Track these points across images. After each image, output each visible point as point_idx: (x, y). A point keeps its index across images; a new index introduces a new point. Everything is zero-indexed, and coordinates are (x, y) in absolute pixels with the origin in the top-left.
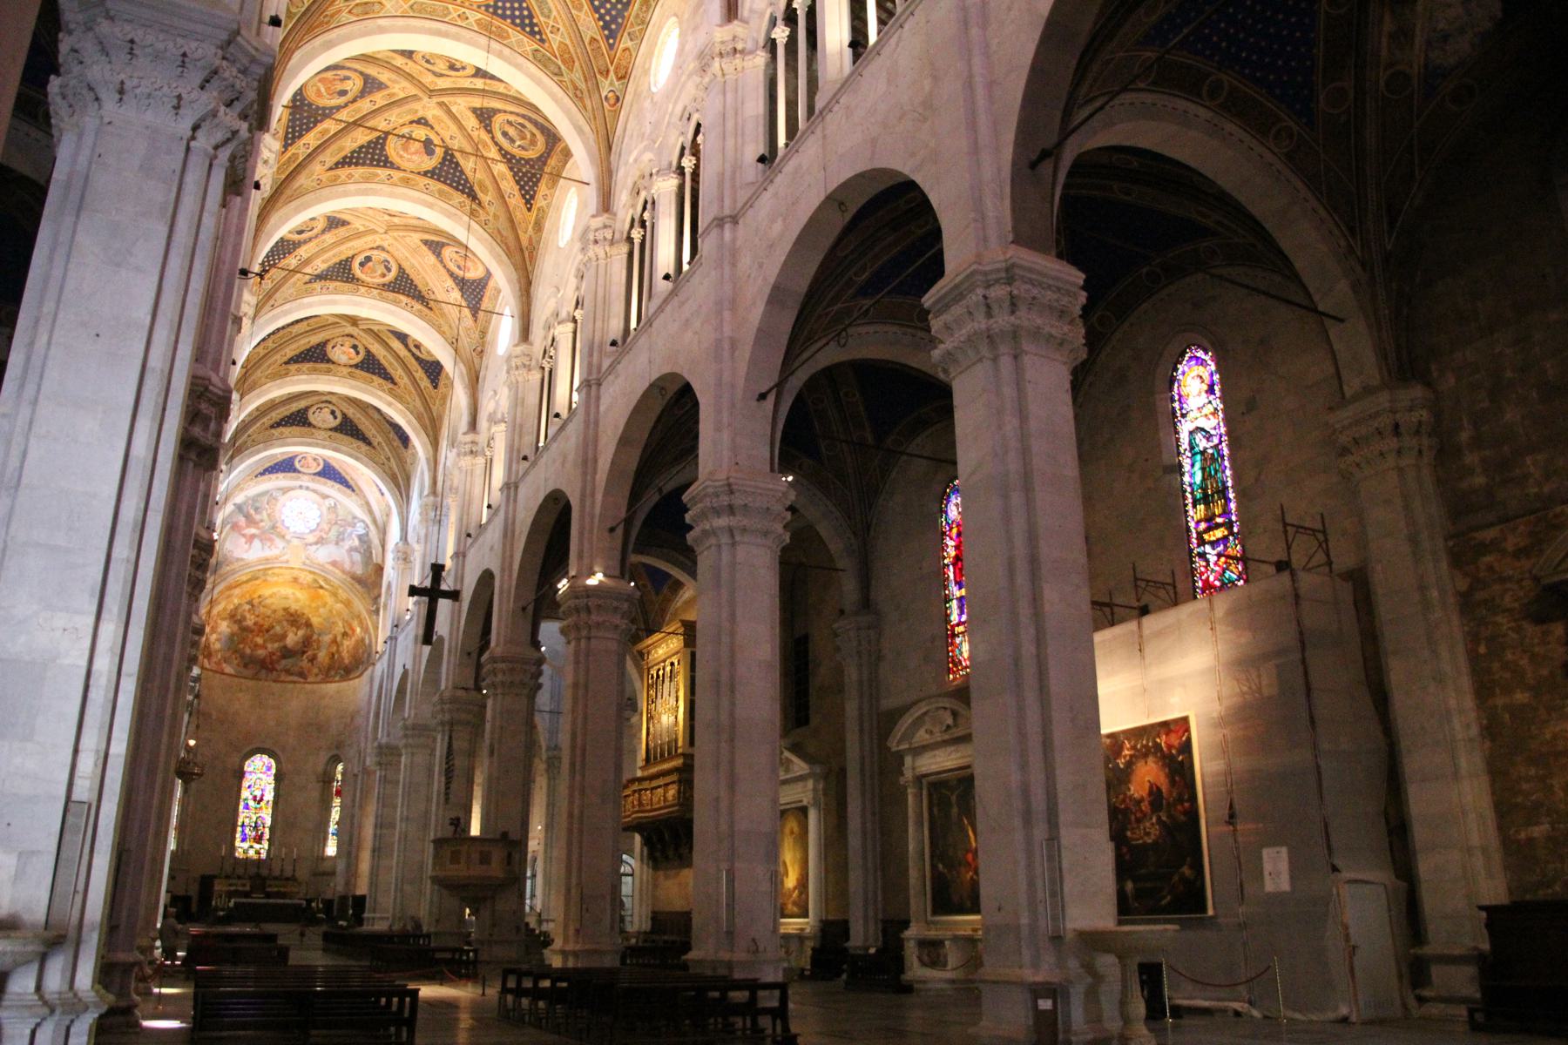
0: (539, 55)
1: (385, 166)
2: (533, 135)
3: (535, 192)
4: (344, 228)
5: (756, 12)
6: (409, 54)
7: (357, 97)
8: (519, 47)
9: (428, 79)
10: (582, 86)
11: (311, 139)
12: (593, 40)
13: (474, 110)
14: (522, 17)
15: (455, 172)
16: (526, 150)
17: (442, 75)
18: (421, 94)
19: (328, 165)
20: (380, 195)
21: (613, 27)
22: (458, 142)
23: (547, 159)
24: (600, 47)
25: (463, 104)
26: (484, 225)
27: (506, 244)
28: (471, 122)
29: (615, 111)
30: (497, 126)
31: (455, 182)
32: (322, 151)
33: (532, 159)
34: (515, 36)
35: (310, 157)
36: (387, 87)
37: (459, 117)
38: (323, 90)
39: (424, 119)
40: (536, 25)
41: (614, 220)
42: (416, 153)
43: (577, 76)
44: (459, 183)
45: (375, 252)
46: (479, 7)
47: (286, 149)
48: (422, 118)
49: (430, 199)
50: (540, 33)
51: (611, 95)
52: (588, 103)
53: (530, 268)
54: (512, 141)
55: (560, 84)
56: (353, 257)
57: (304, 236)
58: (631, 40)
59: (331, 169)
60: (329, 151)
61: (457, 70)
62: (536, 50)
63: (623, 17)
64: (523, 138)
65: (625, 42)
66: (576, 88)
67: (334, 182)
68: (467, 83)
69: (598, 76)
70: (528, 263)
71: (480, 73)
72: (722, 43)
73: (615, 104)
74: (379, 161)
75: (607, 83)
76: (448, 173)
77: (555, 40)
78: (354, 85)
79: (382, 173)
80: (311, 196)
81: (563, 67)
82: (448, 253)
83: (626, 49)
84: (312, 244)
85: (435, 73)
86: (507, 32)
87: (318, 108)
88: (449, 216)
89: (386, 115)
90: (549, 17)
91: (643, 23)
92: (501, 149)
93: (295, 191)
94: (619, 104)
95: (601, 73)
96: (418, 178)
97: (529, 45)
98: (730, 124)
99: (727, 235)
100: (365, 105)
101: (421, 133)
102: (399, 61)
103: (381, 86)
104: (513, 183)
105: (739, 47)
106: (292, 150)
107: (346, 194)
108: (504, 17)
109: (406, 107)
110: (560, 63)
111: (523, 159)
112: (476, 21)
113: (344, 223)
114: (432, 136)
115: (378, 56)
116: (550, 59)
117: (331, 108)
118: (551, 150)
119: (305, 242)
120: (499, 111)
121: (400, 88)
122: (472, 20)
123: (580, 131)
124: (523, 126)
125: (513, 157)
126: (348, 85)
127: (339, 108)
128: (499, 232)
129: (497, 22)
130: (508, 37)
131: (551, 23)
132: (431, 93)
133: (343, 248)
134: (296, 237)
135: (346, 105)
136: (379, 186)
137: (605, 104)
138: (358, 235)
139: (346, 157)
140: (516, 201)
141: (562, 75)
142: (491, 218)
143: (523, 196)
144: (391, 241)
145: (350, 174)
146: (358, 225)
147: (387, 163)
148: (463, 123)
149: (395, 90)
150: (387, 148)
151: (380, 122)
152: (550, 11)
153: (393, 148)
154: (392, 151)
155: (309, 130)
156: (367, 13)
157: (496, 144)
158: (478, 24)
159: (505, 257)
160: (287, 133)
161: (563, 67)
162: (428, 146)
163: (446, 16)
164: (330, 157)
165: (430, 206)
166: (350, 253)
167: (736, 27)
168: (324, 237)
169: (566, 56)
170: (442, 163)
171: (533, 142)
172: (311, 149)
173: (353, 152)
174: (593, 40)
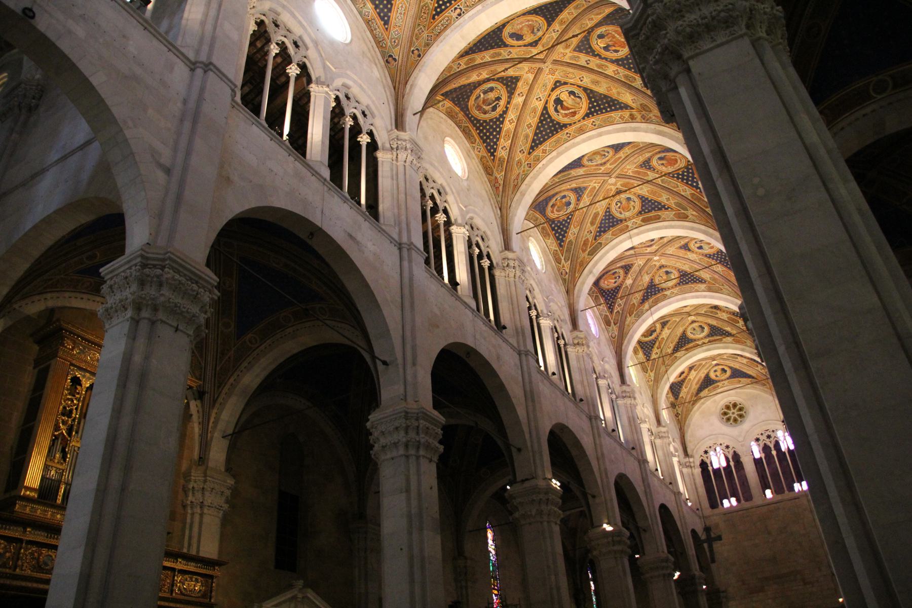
2: (485, 113)
16: (475, 99)
23: (465, 114)
33: (468, 101)
36: (575, 50)
42: (521, 29)
48: (536, 46)
54: (485, 92)
64: (484, 101)
101: (529, 39)
114: (520, 43)
118: (470, 119)
149: (568, 51)
150: (543, 19)
154: (537, 19)
162: (518, 37)
171: (479, 108)
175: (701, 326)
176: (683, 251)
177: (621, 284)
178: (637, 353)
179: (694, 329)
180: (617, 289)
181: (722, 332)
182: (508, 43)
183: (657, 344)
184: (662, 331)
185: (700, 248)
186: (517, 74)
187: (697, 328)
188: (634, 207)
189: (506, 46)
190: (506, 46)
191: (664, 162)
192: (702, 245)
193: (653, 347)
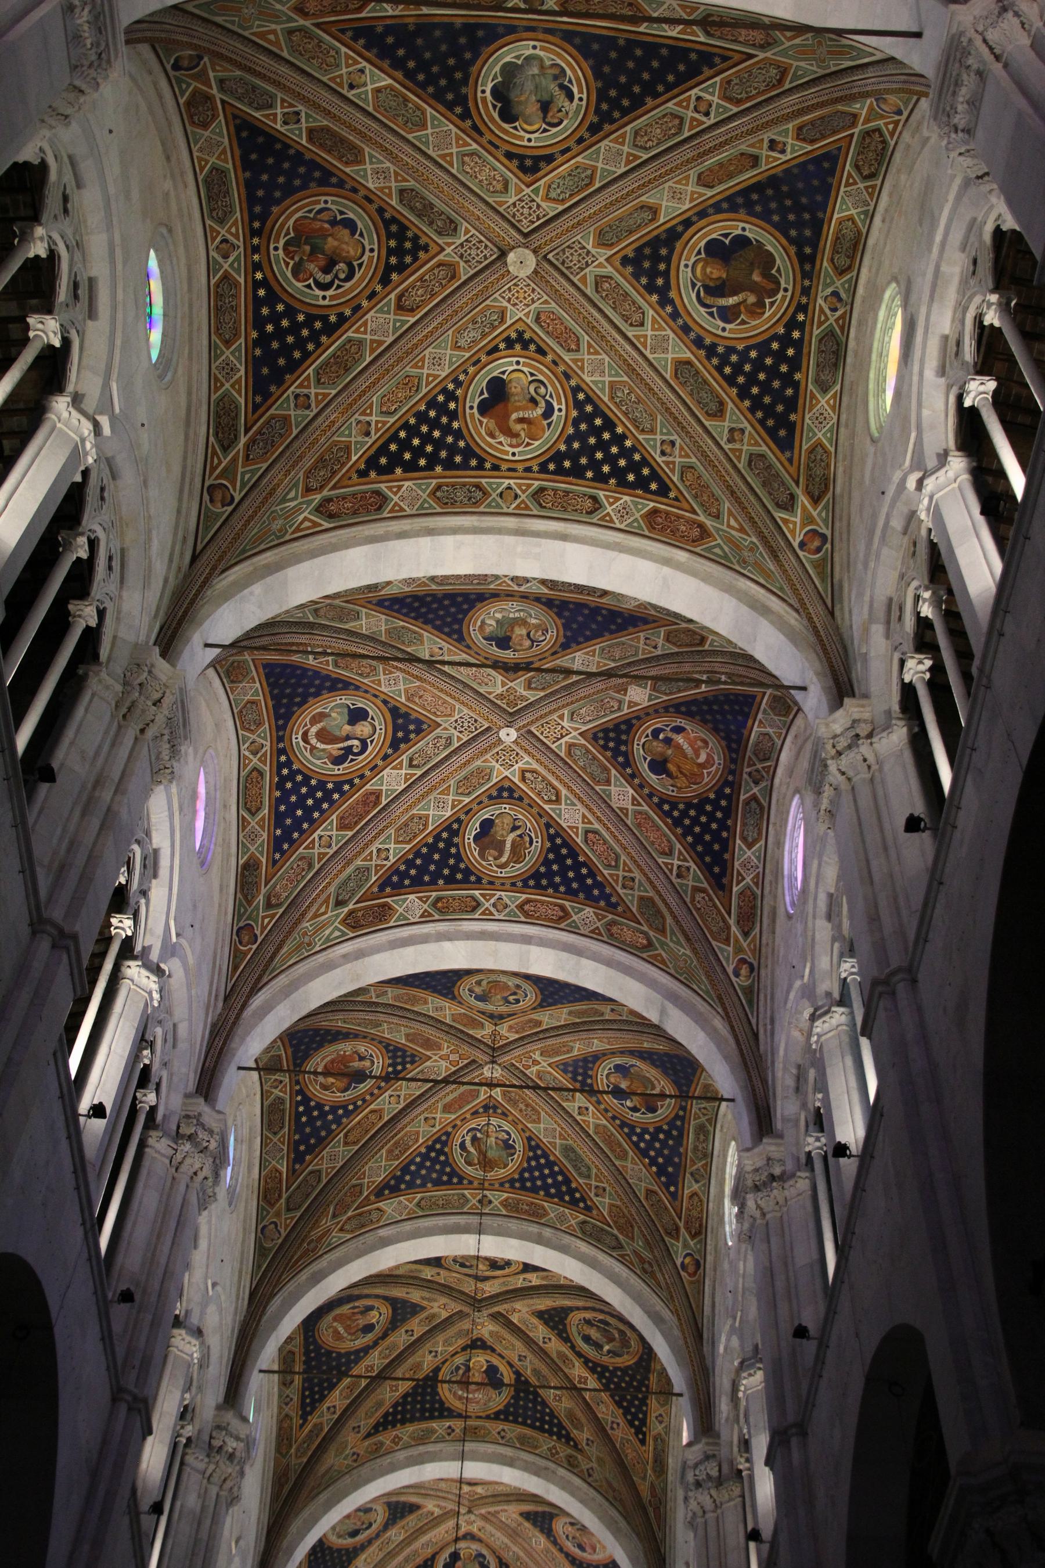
0: (588, 1228)
1: (441, 1416)
2: (622, 1333)
3: (645, 1414)
4: (412, 1517)
5: (789, 1120)
6: (436, 1262)
7: (388, 1329)
8: (562, 1222)
9: (469, 1286)
10: (647, 1255)
11: (337, 1399)
12: (649, 1192)
13: (540, 1315)
14: (556, 1184)
15: (535, 1407)
17: (486, 1279)
18: (466, 1309)
19: (363, 1431)
20: (441, 1460)
21: (670, 1169)
22: (530, 1365)
24: (660, 1200)
25: (525, 1310)
26: (586, 1476)
27: (621, 1501)
28: (540, 1331)
29: (698, 1281)
30: (574, 1329)
31: (538, 1420)
32: (353, 1412)
33: (629, 1367)
34: (553, 1209)
35: (338, 1424)
36: (423, 1308)
37: (523, 1328)
38: (341, 1330)
39: (480, 1339)
40: (576, 1190)
41: (718, 1444)
43: (639, 1244)
44: (543, 1421)
45: (462, 1545)
46: (502, 1185)
47: (305, 1420)
48: (478, 1339)
49: (509, 1452)
50: (583, 1199)
51: (687, 1260)
52: (659, 1275)
53: (659, 1535)
54: (598, 1346)
55: (622, 1260)
56: (433, 1557)
57: (361, 1537)
58: (697, 1181)
59: (369, 1435)
60: (361, 1412)
61: (502, 1268)
62: (584, 1222)
63: (680, 1155)
64: (611, 1340)
65: (690, 1186)
66: (642, 1260)
67: (377, 1452)
68: (519, 1282)
69: (666, 1239)
70: (655, 1527)
71: (528, 1268)
72: (756, 1170)
73: (695, 1273)
74: (432, 1410)
75: (680, 1245)
76: (525, 1408)
77: (603, 1203)
78: (380, 1315)
79: (439, 1426)
80: (347, 1480)
81: (621, 1237)
82: (559, 1526)
83: (694, 1194)
84: (371, 1550)
85: (478, 1278)
86: (543, 1207)
87: (339, 1354)
88: (537, 1472)
89: (428, 1346)
90: (589, 1177)
91: (705, 1156)
92: (586, 1361)
93: (324, 1475)
94: (701, 1270)
95: (669, 1234)
96: (488, 1424)
97: (574, 1218)
98: (780, 1284)
99: (796, 1456)
100: (400, 1339)
101: (480, 1360)
102: (428, 1273)
103: (415, 1309)
104: (612, 1407)
105: (777, 1171)
106: (313, 1420)
107: (393, 1468)
108: (534, 1190)
109: (451, 1331)
110: (615, 1232)
111: (619, 1369)
112: (501, 1203)
113: (413, 1508)
114: (495, 1361)
115: (397, 1272)
116: (602, 1230)
117: (357, 1352)
119: (363, 1547)
120: (571, 1309)
121: (440, 1307)
122: (496, 1203)
123: (657, 1319)
124: (607, 1324)
125: (605, 1368)
126: (373, 1317)
127: (366, 1350)
128: (610, 1485)
129: (526, 1198)
130: (546, 1214)
131: (594, 1183)
132: (477, 1303)
133: (417, 1545)
134: (349, 1541)
135: (376, 1344)
136: (439, 1447)
137: (682, 1273)
138: (436, 1521)
139: (386, 1415)
140: (622, 1433)
141: (621, 1247)
142: (595, 1465)
143: (631, 1423)
144: (480, 1523)
145: (396, 1436)
146: (430, 1506)
147: (444, 1412)
148: (531, 1334)
149: (436, 1310)
151: (424, 1356)
152: (589, 1169)
153: (445, 1392)
155: (332, 1387)
156: (363, 1226)
157: (579, 1355)
158: (505, 1206)
159: (623, 1524)
160: (304, 1397)
161: (621, 1237)
163: (463, 1206)
164: (364, 1419)
165: (510, 1463)
166: (430, 1551)
167: (770, 1147)
168: (388, 1534)
169: (622, 1221)
170: (516, 1397)
171: (625, 1343)
172: (338, 1413)
173: (395, 1406)
174: (649, 1192)
175: (508, 115)
176: (417, 709)
177: (666, 709)
178: (848, 232)
179: (545, 107)
180: (688, 709)
181: (413, 53)
182: (513, 1377)
183: (748, 177)
184: (687, 223)
185: (357, 716)
186: (535, 1321)
187: (532, 108)
188: (479, 983)
189: (518, 1374)
190: (518, 1374)
191: (356, 1064)
192: (347, 728)
193: (773, 181)
